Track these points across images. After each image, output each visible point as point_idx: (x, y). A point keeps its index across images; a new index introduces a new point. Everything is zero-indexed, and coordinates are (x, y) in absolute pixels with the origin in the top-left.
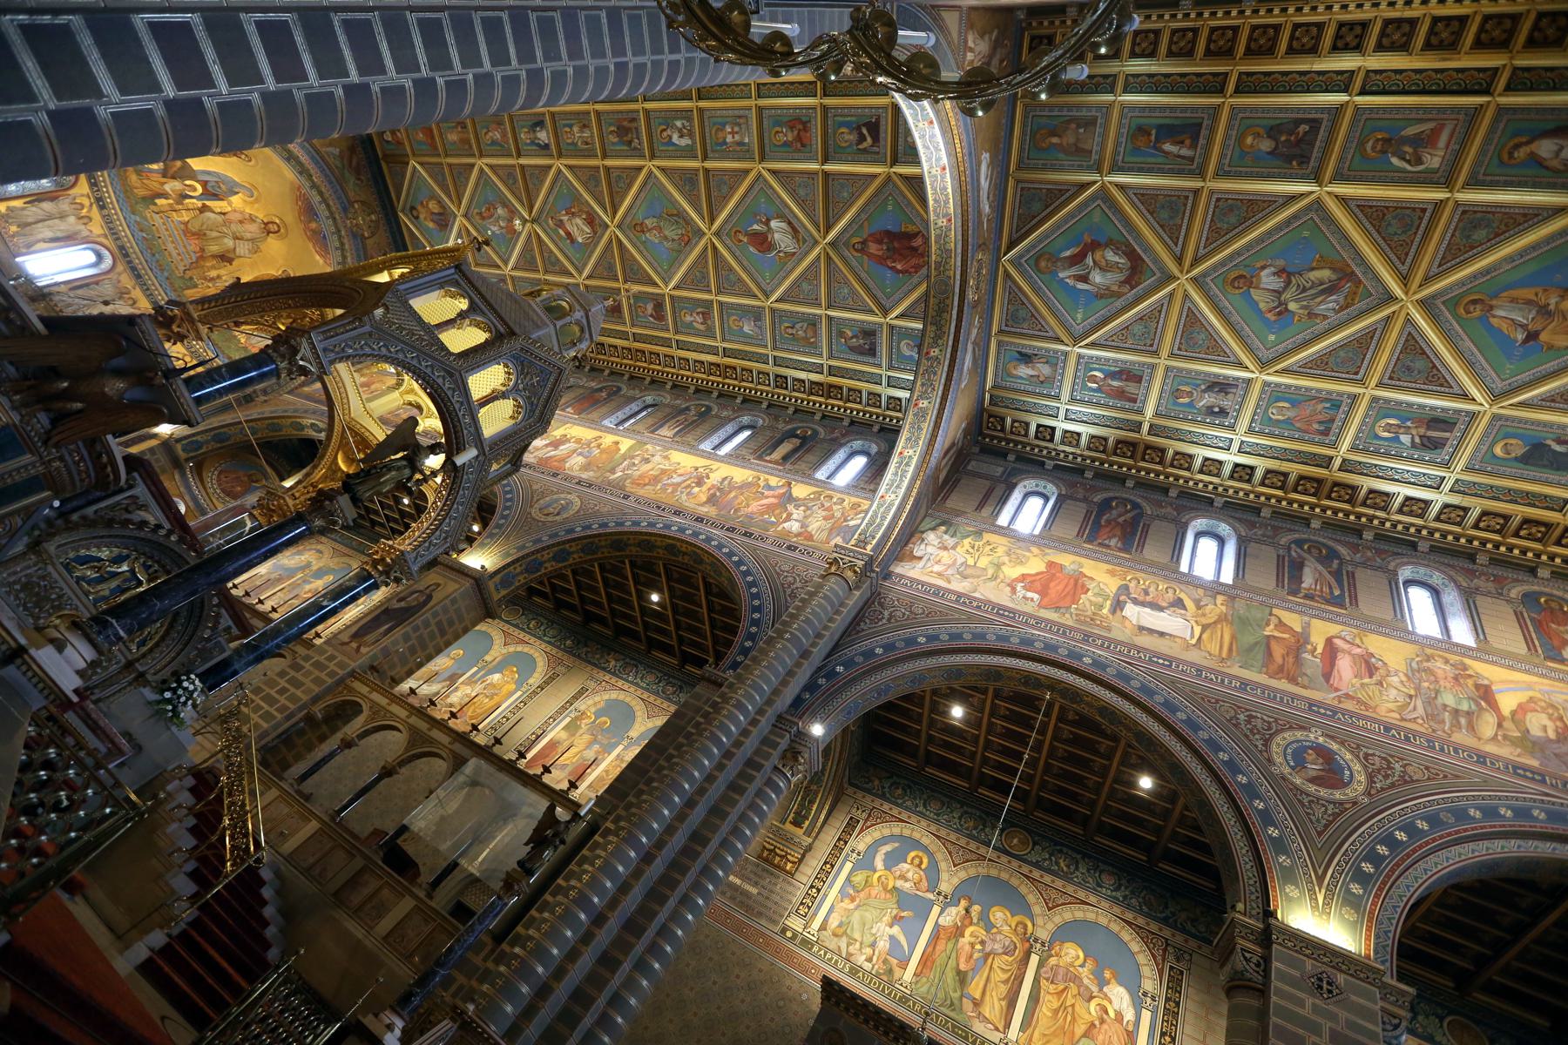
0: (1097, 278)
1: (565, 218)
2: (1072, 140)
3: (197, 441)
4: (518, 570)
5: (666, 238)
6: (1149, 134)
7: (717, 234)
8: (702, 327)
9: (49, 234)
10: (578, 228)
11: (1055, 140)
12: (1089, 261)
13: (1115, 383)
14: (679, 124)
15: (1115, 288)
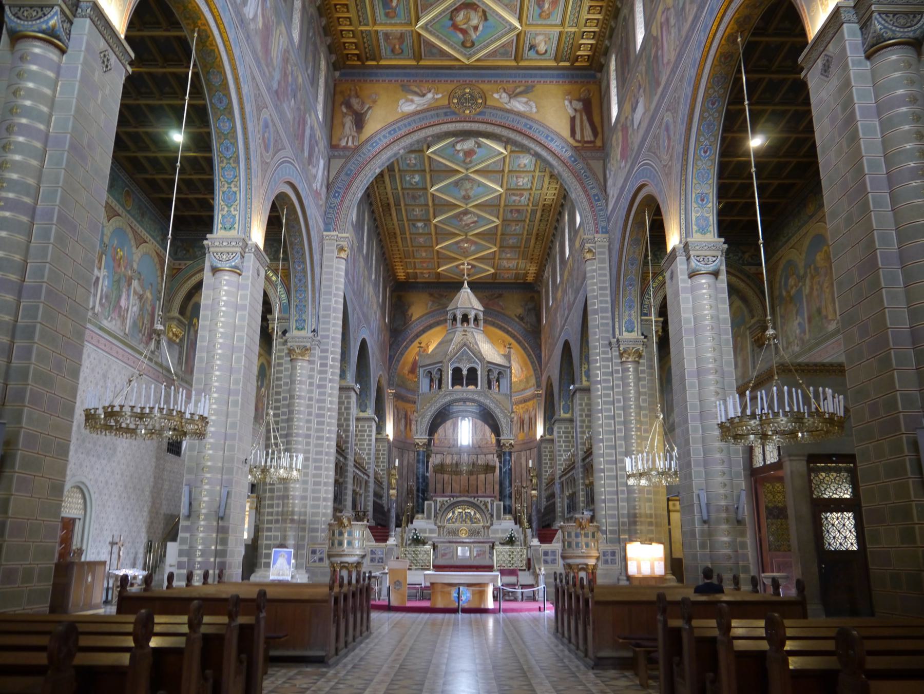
0: (474, 22)
1: (464, 223)
2: (396, 41)
3: (548, 429)
4: (586, 366)
5: (471, 188)
6: (388, 12)
7: (467, 170)
8: (526, 179)
9: (451, 431)
10: (468, 219)
11: (397, 47)
12: (464, 27)
13: (547, 6)
14: (408, 179)
15: (480, 14)
